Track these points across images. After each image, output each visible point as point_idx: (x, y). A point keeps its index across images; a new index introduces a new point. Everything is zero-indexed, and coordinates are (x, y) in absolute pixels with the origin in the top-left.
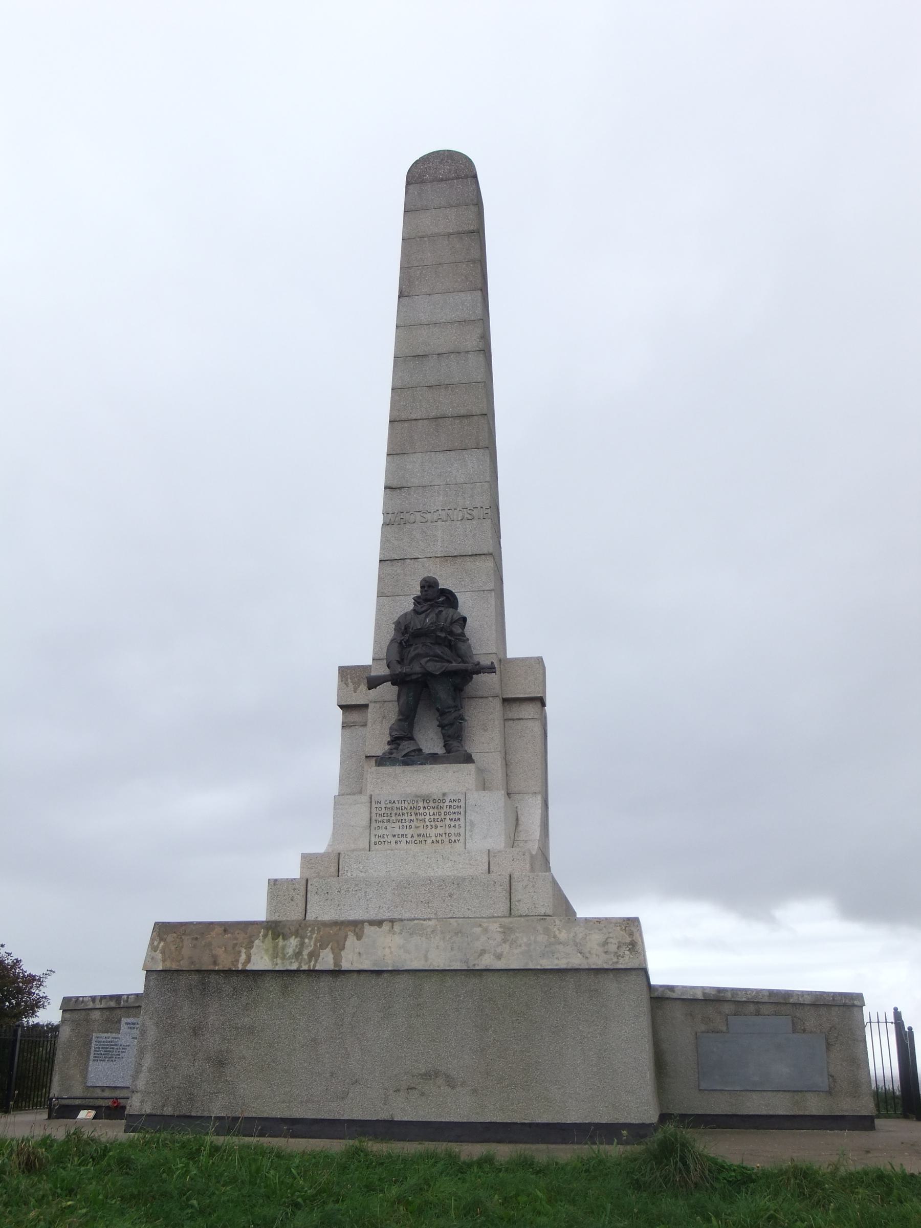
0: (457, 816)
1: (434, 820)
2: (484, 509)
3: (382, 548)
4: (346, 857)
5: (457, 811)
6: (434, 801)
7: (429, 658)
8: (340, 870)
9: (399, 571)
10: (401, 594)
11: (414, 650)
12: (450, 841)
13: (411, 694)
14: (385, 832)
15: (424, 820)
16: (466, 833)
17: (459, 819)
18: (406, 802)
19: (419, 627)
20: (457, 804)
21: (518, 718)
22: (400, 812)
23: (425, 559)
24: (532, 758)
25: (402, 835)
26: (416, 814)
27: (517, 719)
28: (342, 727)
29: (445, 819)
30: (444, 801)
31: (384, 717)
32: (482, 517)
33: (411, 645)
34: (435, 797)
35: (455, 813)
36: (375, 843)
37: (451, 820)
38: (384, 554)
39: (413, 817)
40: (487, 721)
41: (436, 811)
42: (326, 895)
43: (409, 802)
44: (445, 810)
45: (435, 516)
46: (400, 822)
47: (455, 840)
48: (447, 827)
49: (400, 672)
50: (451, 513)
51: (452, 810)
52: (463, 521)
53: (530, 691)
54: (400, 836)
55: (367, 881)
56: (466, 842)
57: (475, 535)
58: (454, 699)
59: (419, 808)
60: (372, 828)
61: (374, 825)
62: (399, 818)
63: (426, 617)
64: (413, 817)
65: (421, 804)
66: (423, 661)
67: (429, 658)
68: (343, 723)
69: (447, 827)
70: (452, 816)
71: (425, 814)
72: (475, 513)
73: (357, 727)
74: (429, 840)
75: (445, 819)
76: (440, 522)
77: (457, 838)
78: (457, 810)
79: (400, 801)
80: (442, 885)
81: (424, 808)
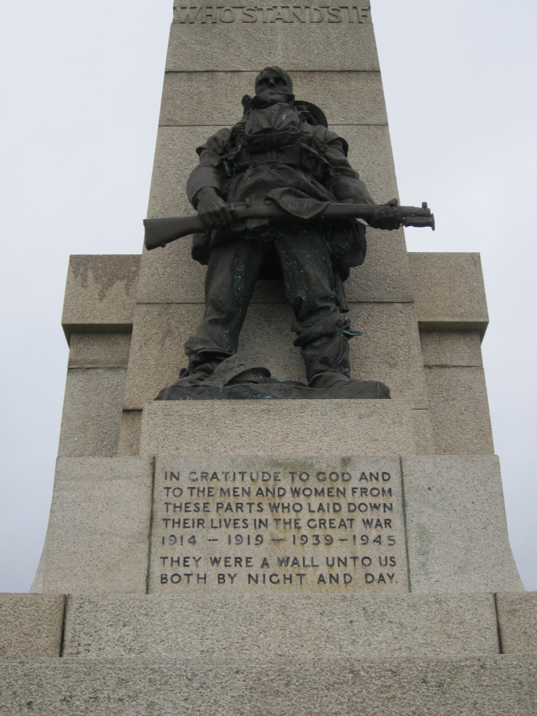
0: (382, 515)
1: (322, 522)
2: (359, 9)
3: (168, 62)
4: (87, 607)
5: (382, 502)
6: (321, 477)
7: (286, 188)
8: (67, 643)
9: (203, 89)
10: (206, 123)
11: (252, 175)
12: (369, 579)
13: (241, 268)
14: (189, 550)
15: (296, 523)
16: (411, 560)
17: (388, 522)
18: (247, 477)
19: (266, 125)
20: (380, 484)
21: (438, 363)
22: (232, 500)
23: (254, 73)
24: (475, 441)
25: (238, 561)
26: (274, 508)
27: (437, 366)
28: (69, 369)
29: (351, 520)
30: (346, 477)
31: (169, 332)
32: (355, 20)
33: (244, 168)
34: (324, 467)
35: (376, 507)
36: (164, 579)
37: (367, 523)
38: (175, 63)
39: (266, 515)
40: (393, 347)
41: (326, 500)
42: (26, 710)
43: (254, 477)
44: (349, 498)
45: (271, 15)
46: (231, 526)
47: (381, 576)
48: (359, 541)
49: (223, 209)
50: (299, 12)
51: (369, 500)
52: (321, 24)
53: (463, 311)
54: (232, 562)
55: (154, 671)
56: (412, 580)
57: (344, 43)
58: (334, 286)
59: (282, 492)
60: (156, 540)
61: (160, 531)
62: (229, 515)
63: (282, 110)
64: (266, 515)
65: (286, 483)
66: (274, 193)
67: (286, 188)
68: (71, 362)
69: (359, 541)
70: (370, 515)
71: (297, 507)
72: (343, 13)
73: (100, 371)
74: (312, 575)
75: (351, 520)
76: (278, 23)
77: (386, 571)
78: (380, 500)
79: (231, 475)
80: (390, 686)
81: (295, 492)
